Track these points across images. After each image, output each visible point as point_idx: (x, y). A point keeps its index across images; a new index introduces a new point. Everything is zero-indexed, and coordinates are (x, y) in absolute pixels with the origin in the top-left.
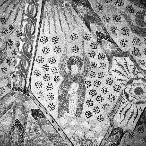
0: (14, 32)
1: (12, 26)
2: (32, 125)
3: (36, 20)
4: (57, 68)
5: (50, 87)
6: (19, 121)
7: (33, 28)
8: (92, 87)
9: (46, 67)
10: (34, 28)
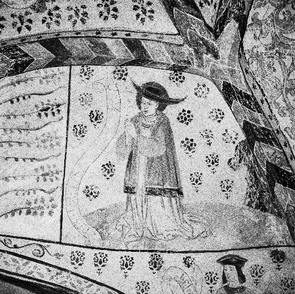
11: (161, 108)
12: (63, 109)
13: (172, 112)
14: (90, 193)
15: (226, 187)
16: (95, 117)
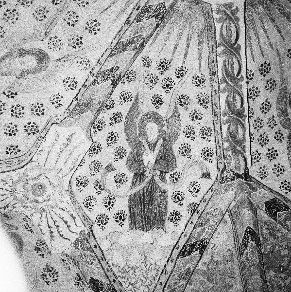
0: (188, 78)
1: (180, 71)
2: (264, 228)
3: (239, 48)
4: (276, 116)
5: (272, 155)
6: (252, 229)
7: (235, 60)
9: (258, 122)
10: (237, 63)
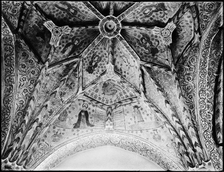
8: (62, 13)
11: (138, 109)
12: (123, 112)
13: (139, 109)
14: (129, 123)
15: (151, 118)
16: (128, 112)
